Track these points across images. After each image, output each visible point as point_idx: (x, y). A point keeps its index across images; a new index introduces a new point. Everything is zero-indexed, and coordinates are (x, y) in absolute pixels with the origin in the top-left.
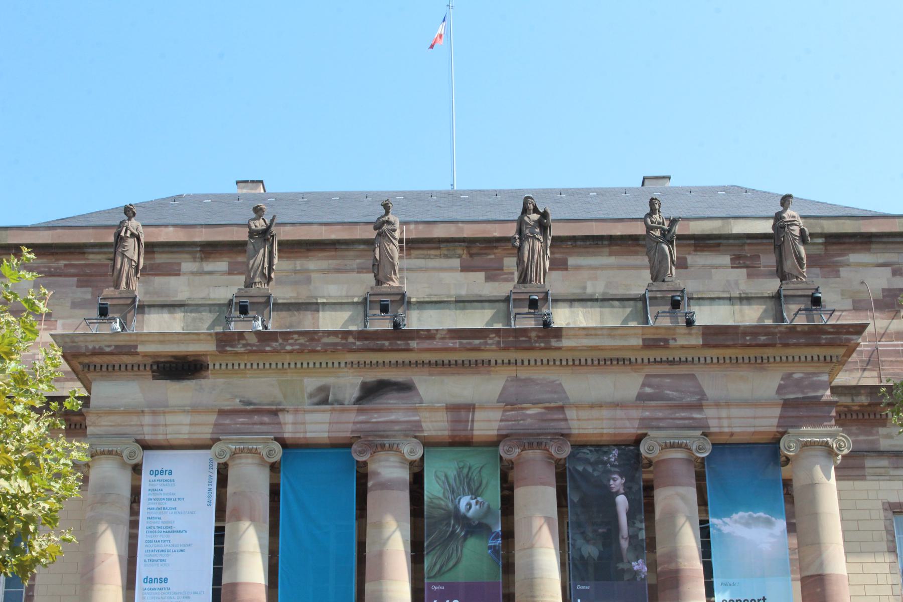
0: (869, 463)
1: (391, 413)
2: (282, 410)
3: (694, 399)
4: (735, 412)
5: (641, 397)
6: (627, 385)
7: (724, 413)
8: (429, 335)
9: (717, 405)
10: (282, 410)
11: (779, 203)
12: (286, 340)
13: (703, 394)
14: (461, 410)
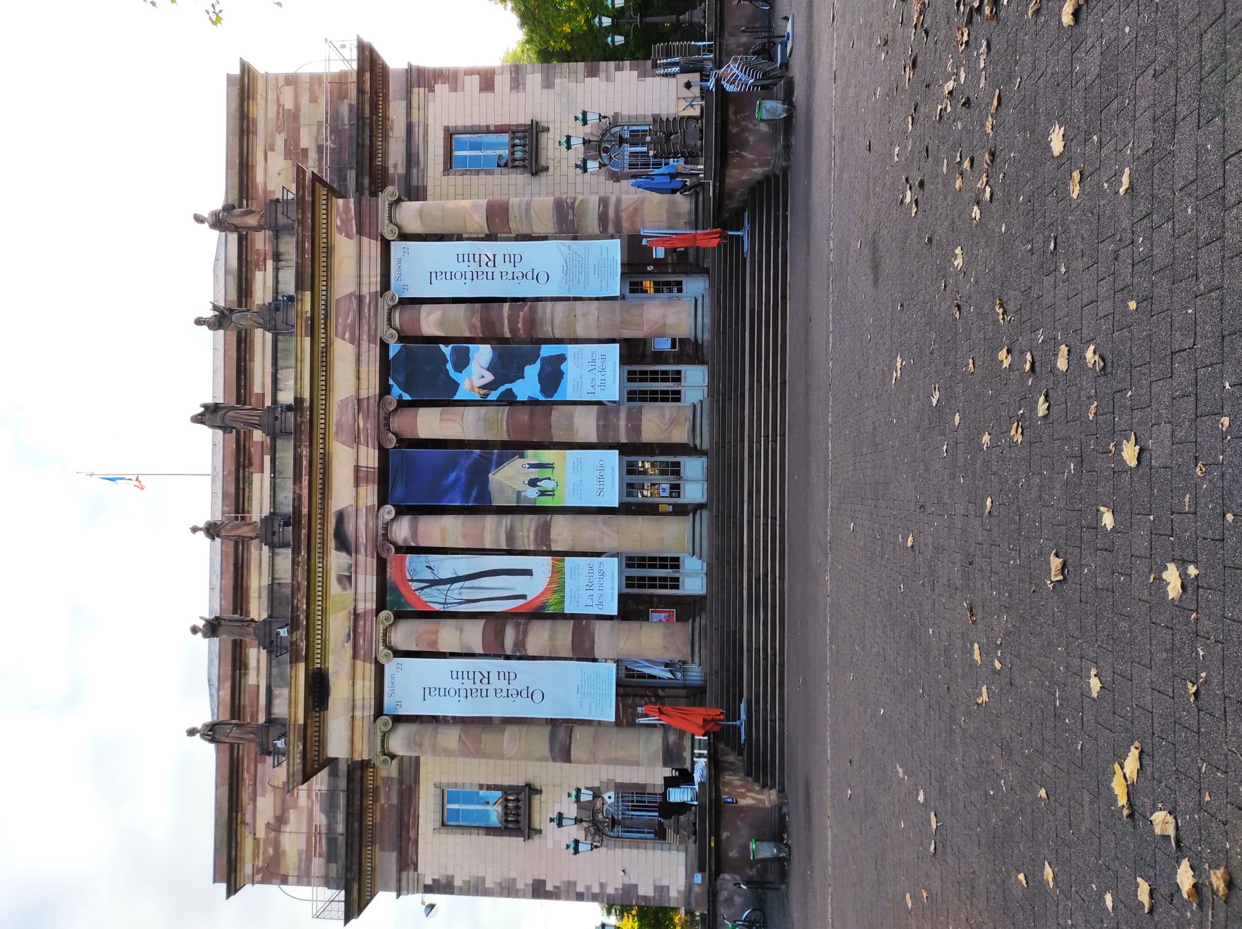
0: (414, 183)
1: (361, 529)
2: (355, 610)
3: (355, 302)
4: (365, 272)
5: (352, 342)
6: (343, 352)
7: (365, 280)
8: (297, 499)
9: (360, 284)
10: (355, 610)
11: (200, 225)
12: (298, 609)
13: (351, 295)
14: (359, 476)
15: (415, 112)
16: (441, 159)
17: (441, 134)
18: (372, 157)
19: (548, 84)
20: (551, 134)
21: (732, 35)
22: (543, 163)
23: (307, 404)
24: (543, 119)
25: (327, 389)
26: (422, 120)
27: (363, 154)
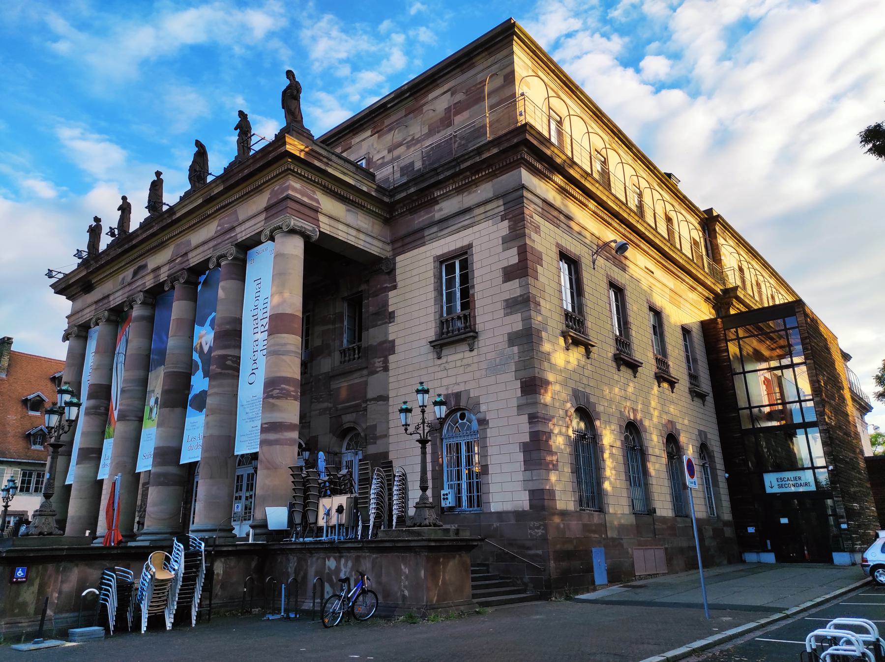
0: (426, 233)
7: (243, 227)
15: (482, 210)
16: (446, 250)
18: (438, 184)
19: (513, 339)
20: (468, 354)
22: (445, 352)
25: (192, 228)
26: (476, 219)
27: (431, 177)
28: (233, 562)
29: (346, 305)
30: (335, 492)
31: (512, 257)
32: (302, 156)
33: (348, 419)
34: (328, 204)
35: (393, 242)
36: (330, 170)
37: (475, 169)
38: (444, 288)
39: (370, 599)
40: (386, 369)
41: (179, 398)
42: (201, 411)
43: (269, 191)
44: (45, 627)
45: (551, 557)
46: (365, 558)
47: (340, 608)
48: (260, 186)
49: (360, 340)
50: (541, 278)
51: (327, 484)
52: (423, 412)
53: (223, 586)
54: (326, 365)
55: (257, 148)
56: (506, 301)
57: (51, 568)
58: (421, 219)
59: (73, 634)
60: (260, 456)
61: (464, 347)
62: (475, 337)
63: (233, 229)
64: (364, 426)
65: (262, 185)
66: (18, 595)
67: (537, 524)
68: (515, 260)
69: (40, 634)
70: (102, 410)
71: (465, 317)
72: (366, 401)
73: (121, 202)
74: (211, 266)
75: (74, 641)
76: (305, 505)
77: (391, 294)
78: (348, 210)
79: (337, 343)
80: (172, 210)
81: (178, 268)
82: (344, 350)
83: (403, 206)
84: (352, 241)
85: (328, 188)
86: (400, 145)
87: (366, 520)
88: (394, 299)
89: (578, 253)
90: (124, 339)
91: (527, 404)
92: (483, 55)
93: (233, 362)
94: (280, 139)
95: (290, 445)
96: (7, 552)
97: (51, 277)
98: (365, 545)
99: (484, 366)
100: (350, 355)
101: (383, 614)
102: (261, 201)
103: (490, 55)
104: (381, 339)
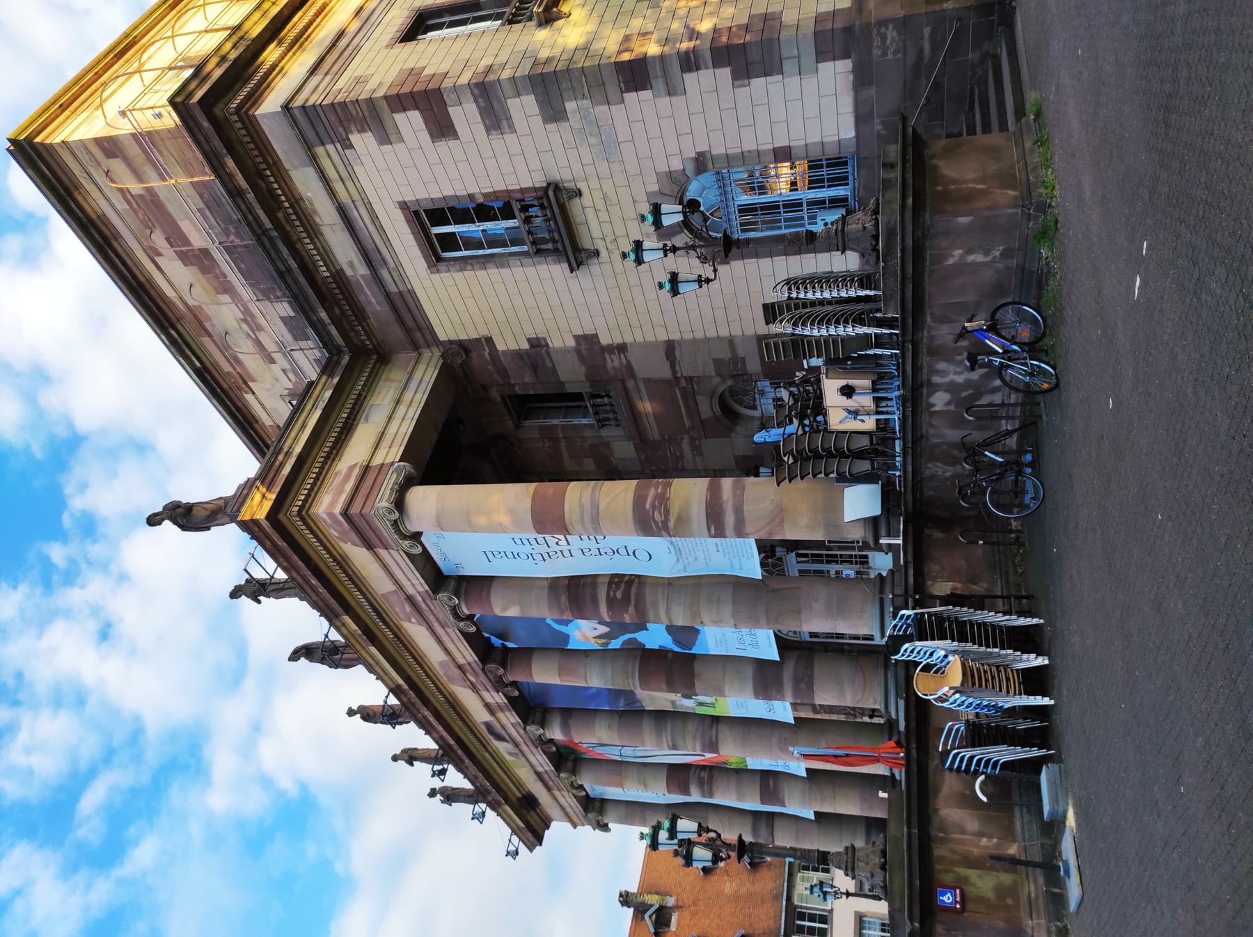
7: (405, 583)
15: (338, 187)
17: (398, 215)
18: (308, 270)
19: (553, 112)
20: (586, 200)
21: (943, 320)
22: (587, 245)
23: (405, 687)
24: (563, 173)
25: (419, 659)
26: (356, 197)
27: (296, 281)
28: (933, 568)
29: (527, 423)
30: (819, 407)
31: (411, 123)
32: (274, 496)
33: (707, 408)
34: (357, 451)
35: (416, 348)
36: (298, 449)
37: (270, 201)
38: (481, 252)
39: (1008, 315)
40: (622, 348)
41: (679, 666)
42: (698, 631)
43: (343, 545)
44: (1038, 858)
45: (937, 8)
46: (932, 338)
47: (1025, 364)
48: (335, 560)
49: (578, 397)
50: (443, 68)
51: (807, 422)
52: (674, 249)
53: (974, 580)
54: (623, 449)
55: (270, 564)
56: (488, 130)
57: (938, 851)
58: (371, 299)
59: (1052, 813)
60: (763, 535)
61: (575, 206)
62: (555, 187)
63: (410, 599)
64: (717, 380)
65: (332, 556)
66: (982, 900)
67: (877, 42)
68: (415, 115)
69: (1051, 868)
70: (704, 774)
71: (525, 209)
72: (676, 379)
73: (401, 763)
74: (473, 629)
75: (1065, 812)
76: (841, 454)
77: (501, 347)
78: (367, 420)
79: (588, 433)
80: (395, 690)
81: (483, 678)
82: (599, 421)
83: (354, 332)
84: (415, 412)
85: (330, 453)
86: (258, 343)
87: (865, 341)
88: (509, 341)
89: (406, 13)
90: (600, 750)
91: (666, 77)
92: (79, 198)
93: (618, 589)
94: (250, 527)
95: (743, 488)
96: (911, 919)
97: (517, 853)
98: (909, 337)
99: (603, 168)
100: (607, 412)
101: (1034, 292)
102: (359, 556)
103: (78, 186)
104: (575, 360)
